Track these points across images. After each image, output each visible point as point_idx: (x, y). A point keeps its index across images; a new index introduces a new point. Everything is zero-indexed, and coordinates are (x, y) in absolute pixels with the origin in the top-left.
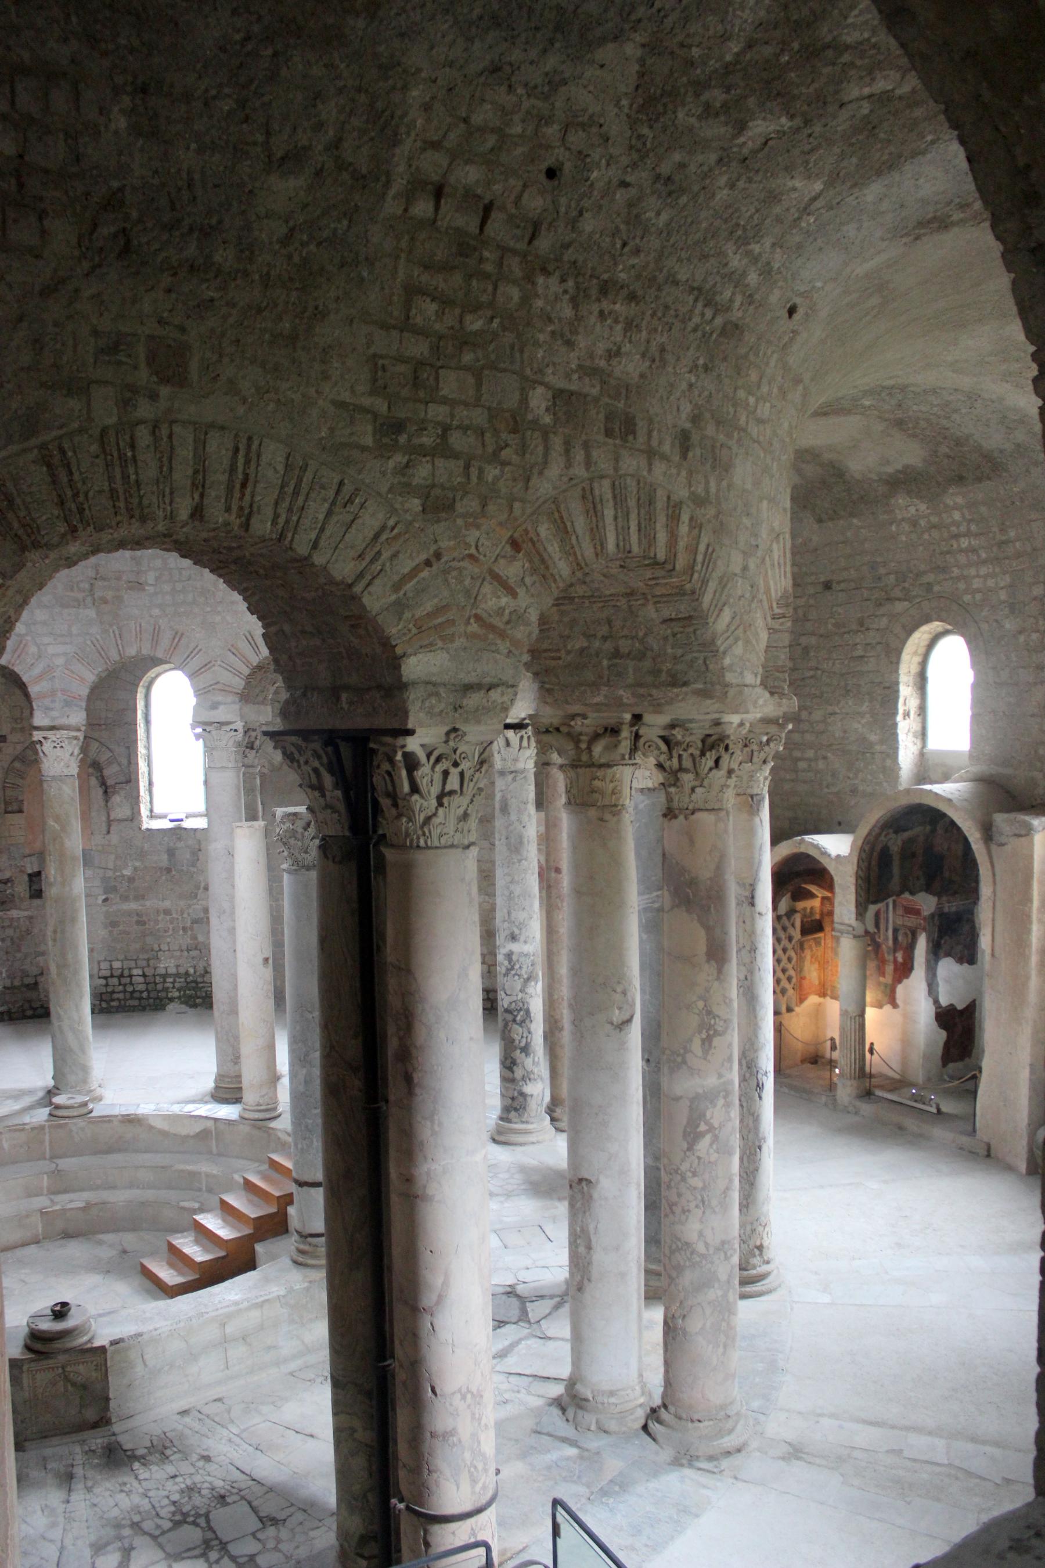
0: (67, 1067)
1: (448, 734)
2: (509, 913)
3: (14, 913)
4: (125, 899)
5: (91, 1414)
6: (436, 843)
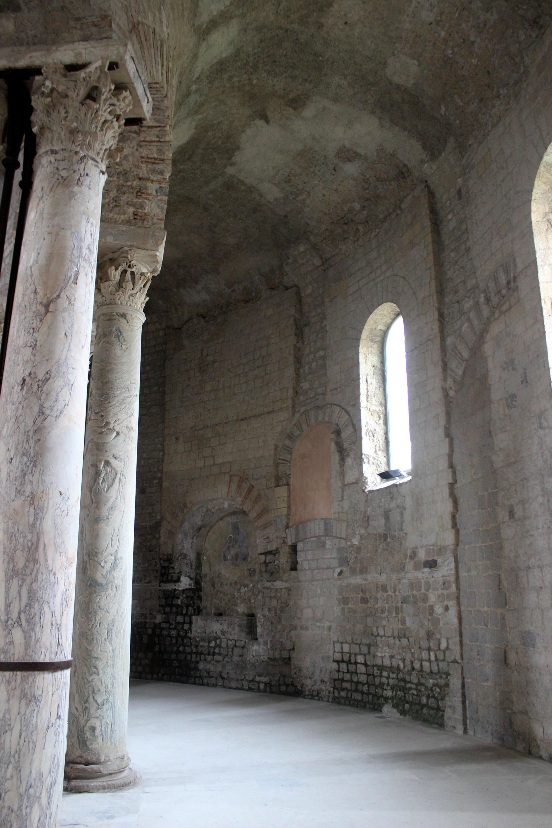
3: (279, 584)
4: (353, 572)
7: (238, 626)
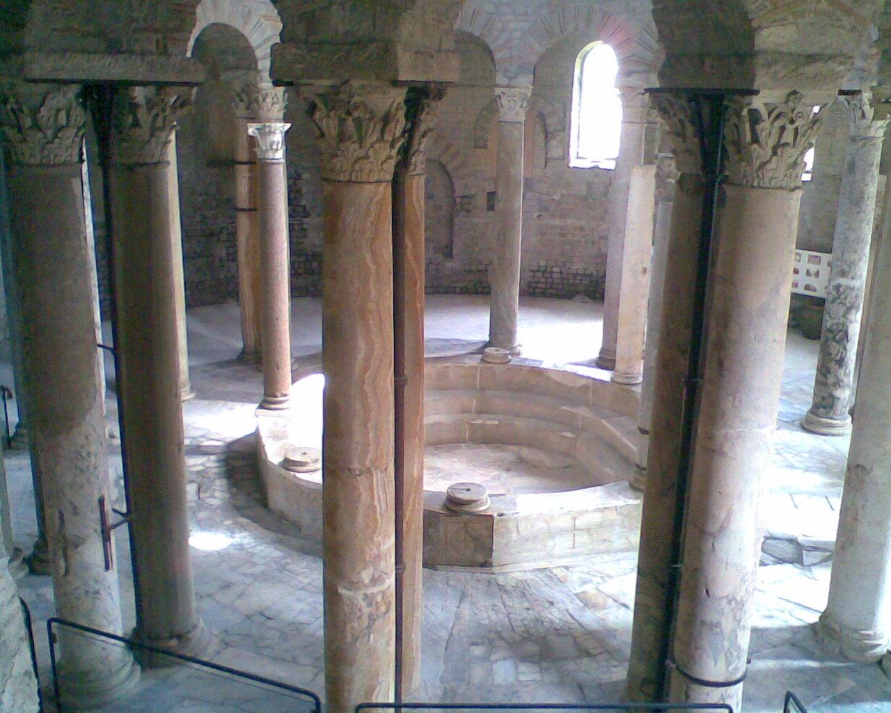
0: (501, 332)
1: (788, 96)
2: (843, 254)
4: (553, 216)
5: (480, 558)
6: (767, 185)
7: (433, 249)
